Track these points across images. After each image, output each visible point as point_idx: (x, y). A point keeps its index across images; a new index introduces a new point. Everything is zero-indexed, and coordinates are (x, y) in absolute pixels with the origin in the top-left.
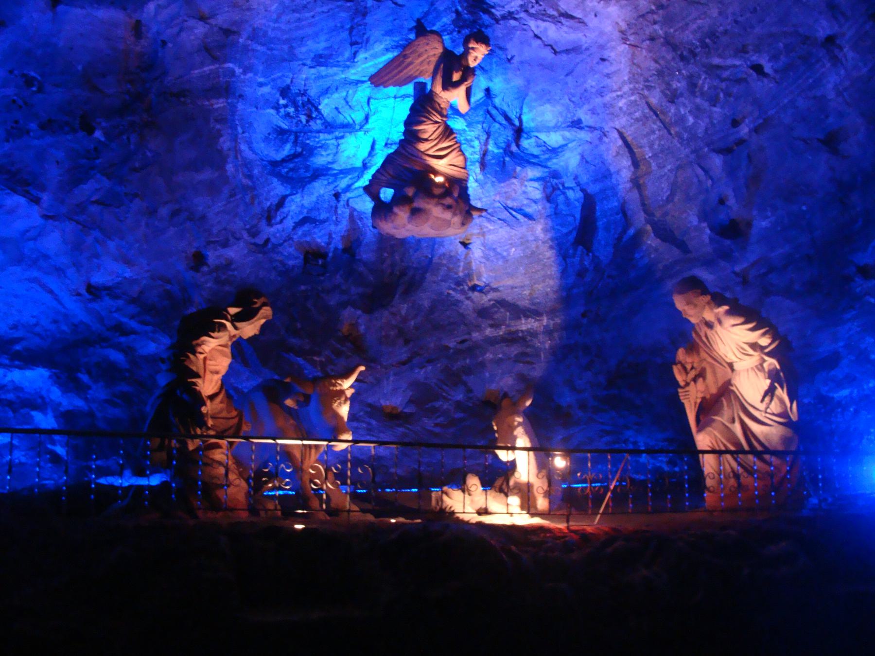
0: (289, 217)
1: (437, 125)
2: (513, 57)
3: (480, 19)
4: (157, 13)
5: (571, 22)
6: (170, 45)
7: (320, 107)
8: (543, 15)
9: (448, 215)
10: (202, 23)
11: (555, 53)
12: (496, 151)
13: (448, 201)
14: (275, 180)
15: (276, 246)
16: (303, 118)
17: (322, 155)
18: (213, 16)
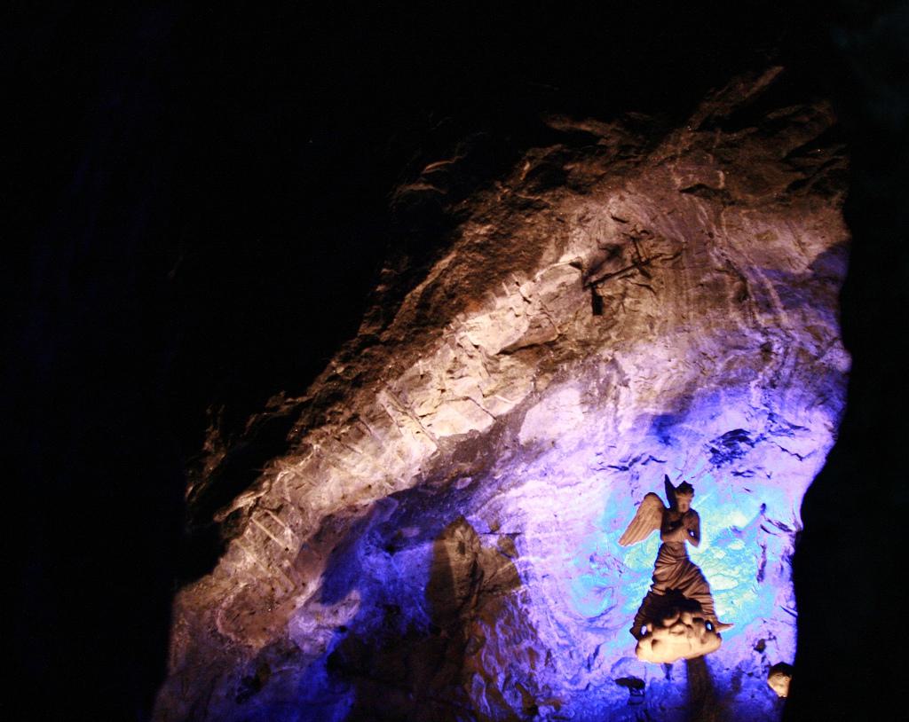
0: (606, 661)
1: (674, 566)
2: (771, 473)
3: (739, 448)
4: (464, 536)
5: (797, 432)
6: (480, 555)
7: (624, 562)
8: (780, 431)
9: (683, 639)
10: (491, 535)
11: (801, 459)
12: (774, 559)
13: (679, 628)
14: (589, 634)
15: (596, 688)
16: (617, 574)
17: (633, 602)
18: (498, 527)
